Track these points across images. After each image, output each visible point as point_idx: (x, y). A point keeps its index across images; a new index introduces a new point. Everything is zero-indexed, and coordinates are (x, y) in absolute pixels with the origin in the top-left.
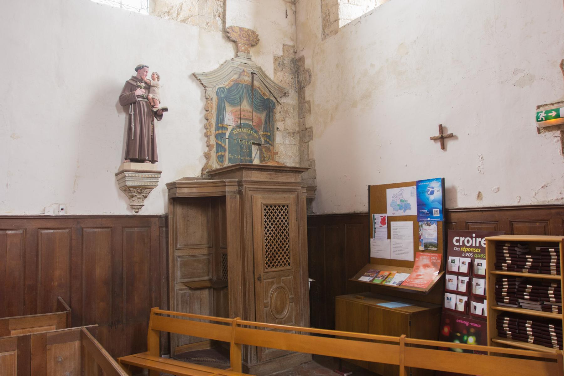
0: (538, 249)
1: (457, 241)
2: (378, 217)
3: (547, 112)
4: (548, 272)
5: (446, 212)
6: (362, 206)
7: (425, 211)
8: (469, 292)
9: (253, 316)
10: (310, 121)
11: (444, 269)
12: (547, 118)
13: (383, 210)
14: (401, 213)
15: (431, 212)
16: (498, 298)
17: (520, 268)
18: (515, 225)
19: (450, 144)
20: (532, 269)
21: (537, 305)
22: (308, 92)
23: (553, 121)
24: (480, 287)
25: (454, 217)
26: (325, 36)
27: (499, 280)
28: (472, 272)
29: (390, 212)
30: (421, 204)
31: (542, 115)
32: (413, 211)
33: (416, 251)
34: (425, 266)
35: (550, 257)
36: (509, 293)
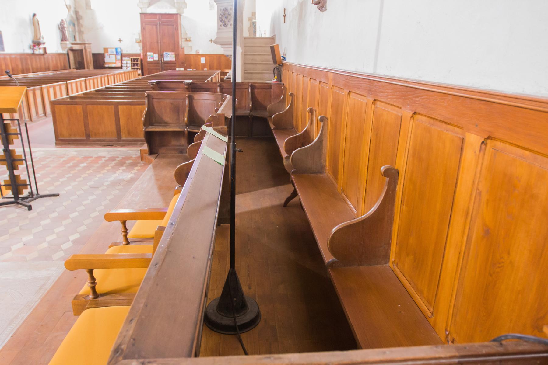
1: (124, 58)
2: (106, 55)
5: (122, 54)
6: (101, 51)
7: (117, 53)
8: (127, 67)
9: (133, 59)
10: (82, 29)
11: (122, 63)
13: (108, 52)
14: (112, 53)
15: (118, 54)
16: (132, 66)
19: (121, 42)
22: (81, 21)
24: (129, 65)
25: (123, 55)
26: (87, 9)
27: (132, 64)
28: (127, 63)
29: (109, 53)
30: (117, 52)
32: (115, 53)
33: (116, 61)
34: (118, 63)
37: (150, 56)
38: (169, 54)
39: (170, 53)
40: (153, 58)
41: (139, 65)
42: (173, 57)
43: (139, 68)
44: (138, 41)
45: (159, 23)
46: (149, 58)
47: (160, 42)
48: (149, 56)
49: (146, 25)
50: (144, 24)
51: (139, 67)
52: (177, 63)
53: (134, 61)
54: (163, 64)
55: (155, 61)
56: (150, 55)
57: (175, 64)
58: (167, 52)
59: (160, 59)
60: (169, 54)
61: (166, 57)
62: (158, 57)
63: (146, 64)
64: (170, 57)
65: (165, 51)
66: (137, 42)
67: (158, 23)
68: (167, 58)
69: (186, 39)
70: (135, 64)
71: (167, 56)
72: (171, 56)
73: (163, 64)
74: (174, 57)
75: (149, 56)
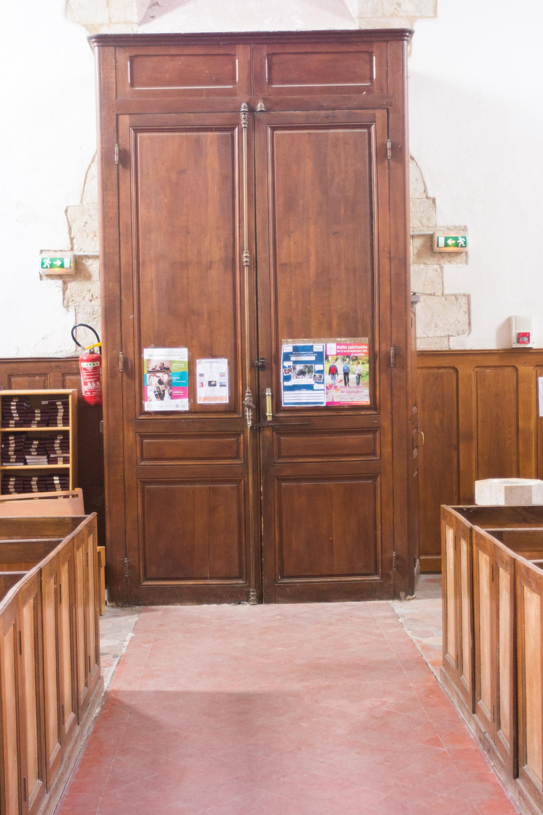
0: (44, 403)
3: (52, 260)
4: (56, 424)
12: (52, 266)
17: (27, 422)
18: (13, 379)
20: (39, 424)
21: (44, 459)
23: (57, 271)
31: (47, 262)
35: (56, 410)
36: (16, 451)
37: (165, 378)
38: (321, 357)
39: (332, 348)
40: (192, 393)
41: (64, 447)
42: (352, 377)
43: (63, 474)
44: (57, 271)
45: (252, 110)
46: (160, 396)
47: (254, 265)
48: (154, 372)
49: (137, 131)
50: (125, 120)
51: (60, 465)
52: (386, 424)
53: (25, 421)
54: (268, 433)
55: (207, 409)
56: (165, 369)
57: (373, 430)
58: (301, 343)
59: (248, 400)
60: (321, 357)
61: (294, 381)
62: (226, 380)
63: (130, 436)
64: (328, 378)
65: (292, 336)
66: (51, 276)
67: (244, 107)
68: (309, 387)
69: (431, 238)
70: (30, 437)
71: (302, 373)
72: (340, 366)
73: (268, 433)
74: (366, 380)
75: (154, 372)
